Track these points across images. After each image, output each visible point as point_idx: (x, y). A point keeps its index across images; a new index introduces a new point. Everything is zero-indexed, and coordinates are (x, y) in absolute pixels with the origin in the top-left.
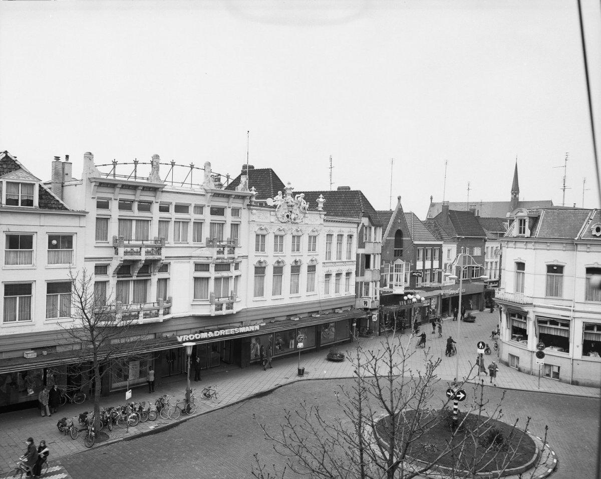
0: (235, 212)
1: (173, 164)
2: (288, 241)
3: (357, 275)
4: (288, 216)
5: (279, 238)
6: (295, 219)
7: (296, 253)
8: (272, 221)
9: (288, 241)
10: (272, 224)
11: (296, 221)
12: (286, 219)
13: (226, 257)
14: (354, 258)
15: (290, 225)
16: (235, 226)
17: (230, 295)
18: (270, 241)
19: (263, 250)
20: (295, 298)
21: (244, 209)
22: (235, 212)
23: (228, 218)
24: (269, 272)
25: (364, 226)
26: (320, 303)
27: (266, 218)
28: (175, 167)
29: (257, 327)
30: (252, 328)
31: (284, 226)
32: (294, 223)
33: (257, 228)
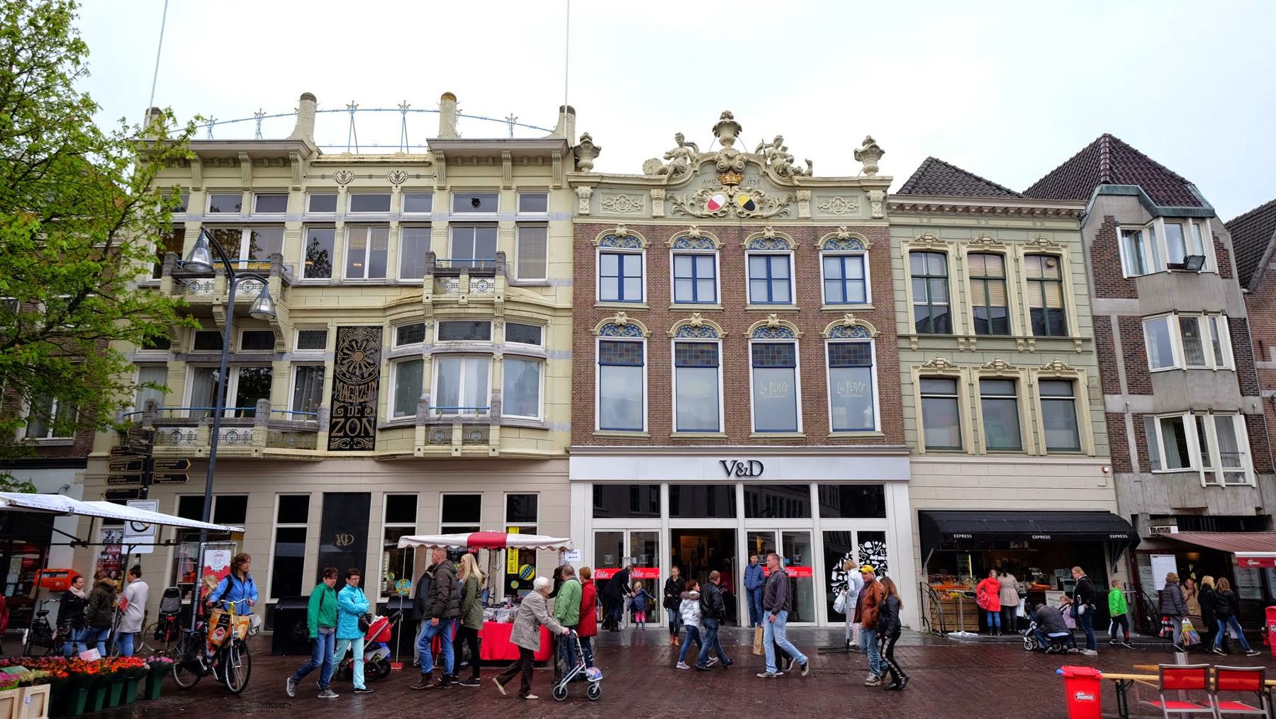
0: (533, 199)
3: (1108, 384)
6: (750, 206)
11: (757, 212)
21: (557, 188)
22: (533, 199)
23: (508, 210)
25: (1116, 224)
27: (638, 208)
28: (356, 114)
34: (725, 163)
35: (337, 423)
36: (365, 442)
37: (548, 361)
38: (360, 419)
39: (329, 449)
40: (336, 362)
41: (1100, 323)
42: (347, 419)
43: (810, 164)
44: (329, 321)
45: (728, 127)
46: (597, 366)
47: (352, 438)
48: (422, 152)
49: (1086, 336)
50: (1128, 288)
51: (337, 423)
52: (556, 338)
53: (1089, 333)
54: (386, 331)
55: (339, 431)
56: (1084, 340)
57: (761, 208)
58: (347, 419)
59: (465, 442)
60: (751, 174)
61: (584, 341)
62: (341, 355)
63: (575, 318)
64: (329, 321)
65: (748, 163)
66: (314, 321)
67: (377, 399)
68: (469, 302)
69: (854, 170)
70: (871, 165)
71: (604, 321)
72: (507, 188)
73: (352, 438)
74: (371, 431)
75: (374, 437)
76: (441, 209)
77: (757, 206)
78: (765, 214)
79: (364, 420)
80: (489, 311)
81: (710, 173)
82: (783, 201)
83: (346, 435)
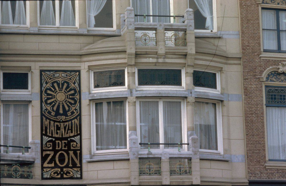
35: (49, 155)
36: (73, 172)
37: (225, 103)
38: (67, 152)
39: (43, 178)
40: (41, 102)
42: (56, 152)
44: (32, 64)
46: (265, 107)
47: (62, 169)
51: (48, 155)
52: (229, 82)
54: (84, 75)
55: (50, 162)
58: (56, 152)
59: (172, 172)
61: (254, 86)
62: (46, 95)
63: (245, 67)
64: (32, 64)
66: (16, 65)
67: (80, 134)
68: (166, 53)
71: (270, 69)
73: (62, 169)
74: (77, 162)
75: (81, 167)
79: (71, 153)
80: (182, 61)
83: (56, 166)
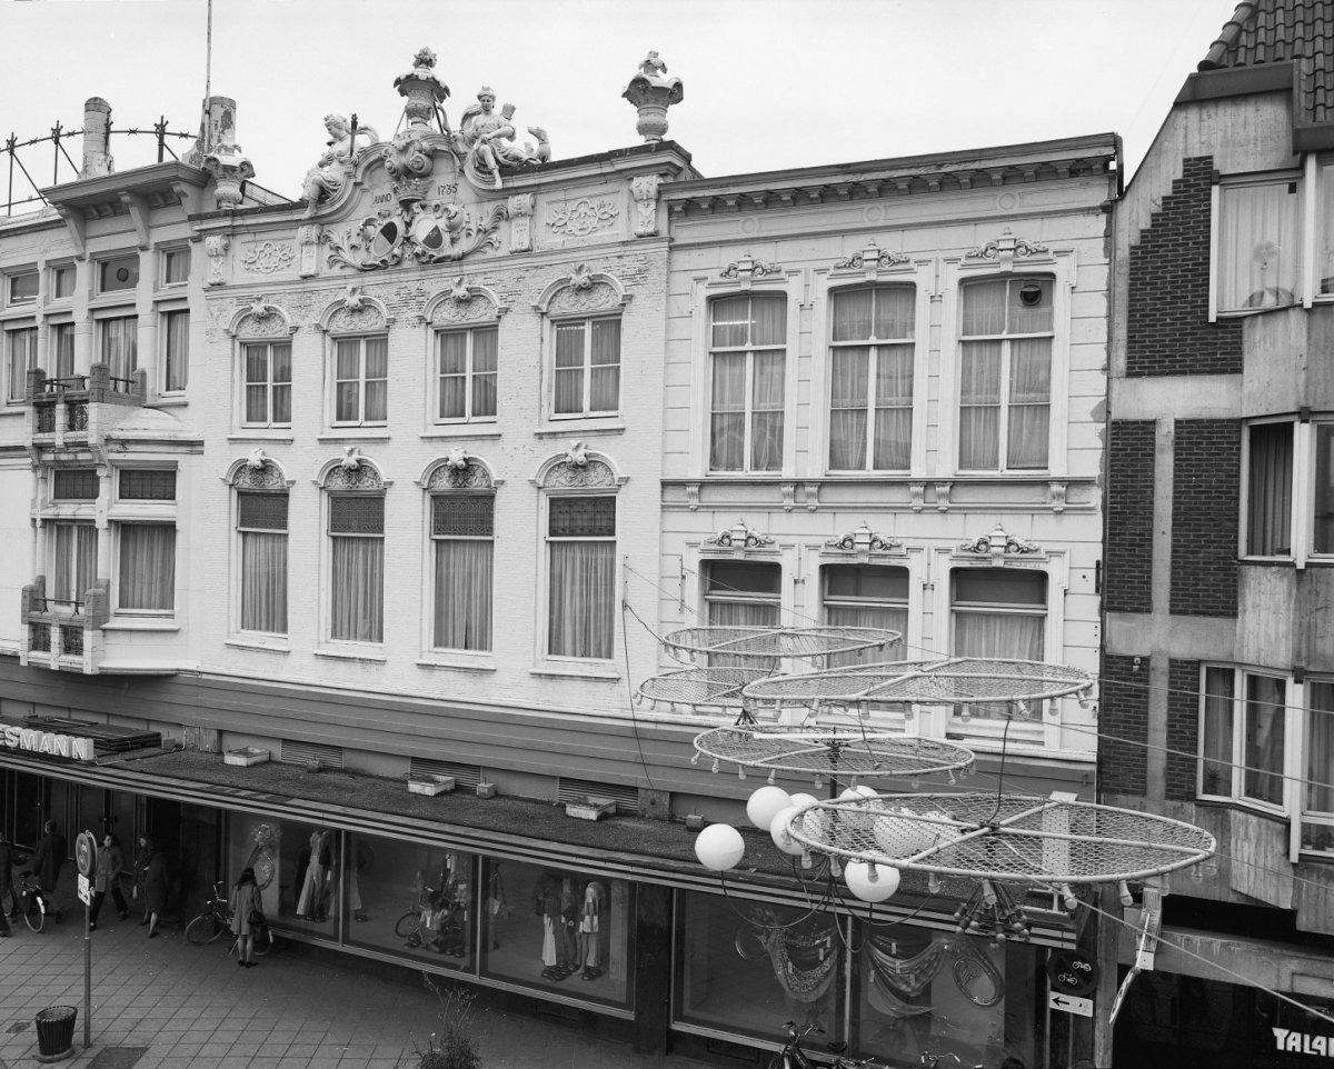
1: (12, 146)
2: (413, 361)
3: (1121, 586)
4: (389, 232)
5: (363, 349)
6: (434, 240)
7: (473, 425)
8: (309, 269)
9: (413, 361)
10: (311, 285)
11: (447, 250)
12: (380, 250)
13: (59, 442)
14: (1077, 450)
15: (411, 279)
16: (174, 316)
17: (74, 598)
18: (312, 369)
19: (282, 415)
20: (451, 675)
24: (308, 518)
26: (637, 736)
29: (82, 748)
30: (56, 744)
31: (379, 289)
32: (432, 258)
33: (233, 310)
34: (396, 161)
41: (1128, 443)
43: (538, 134)
45: (421, 88)
48: (37, 210)
49: (1080, 472)
50: (1218, 348)
53: (1090, 463)
56: (1071, 483)
57: (453, 241)
60: (444, 176)
65: (433, 155)
69: (621, 128)
70: (652, 119)
72: (144, 248)
76: (81, 298)
77: (446, 238)
78: (456, 251)
81: (384, 185)
82: (487, 223)
